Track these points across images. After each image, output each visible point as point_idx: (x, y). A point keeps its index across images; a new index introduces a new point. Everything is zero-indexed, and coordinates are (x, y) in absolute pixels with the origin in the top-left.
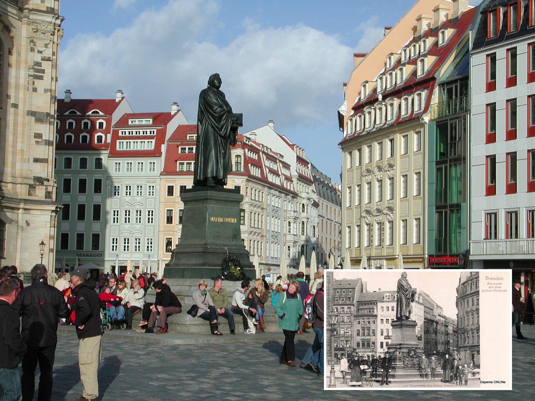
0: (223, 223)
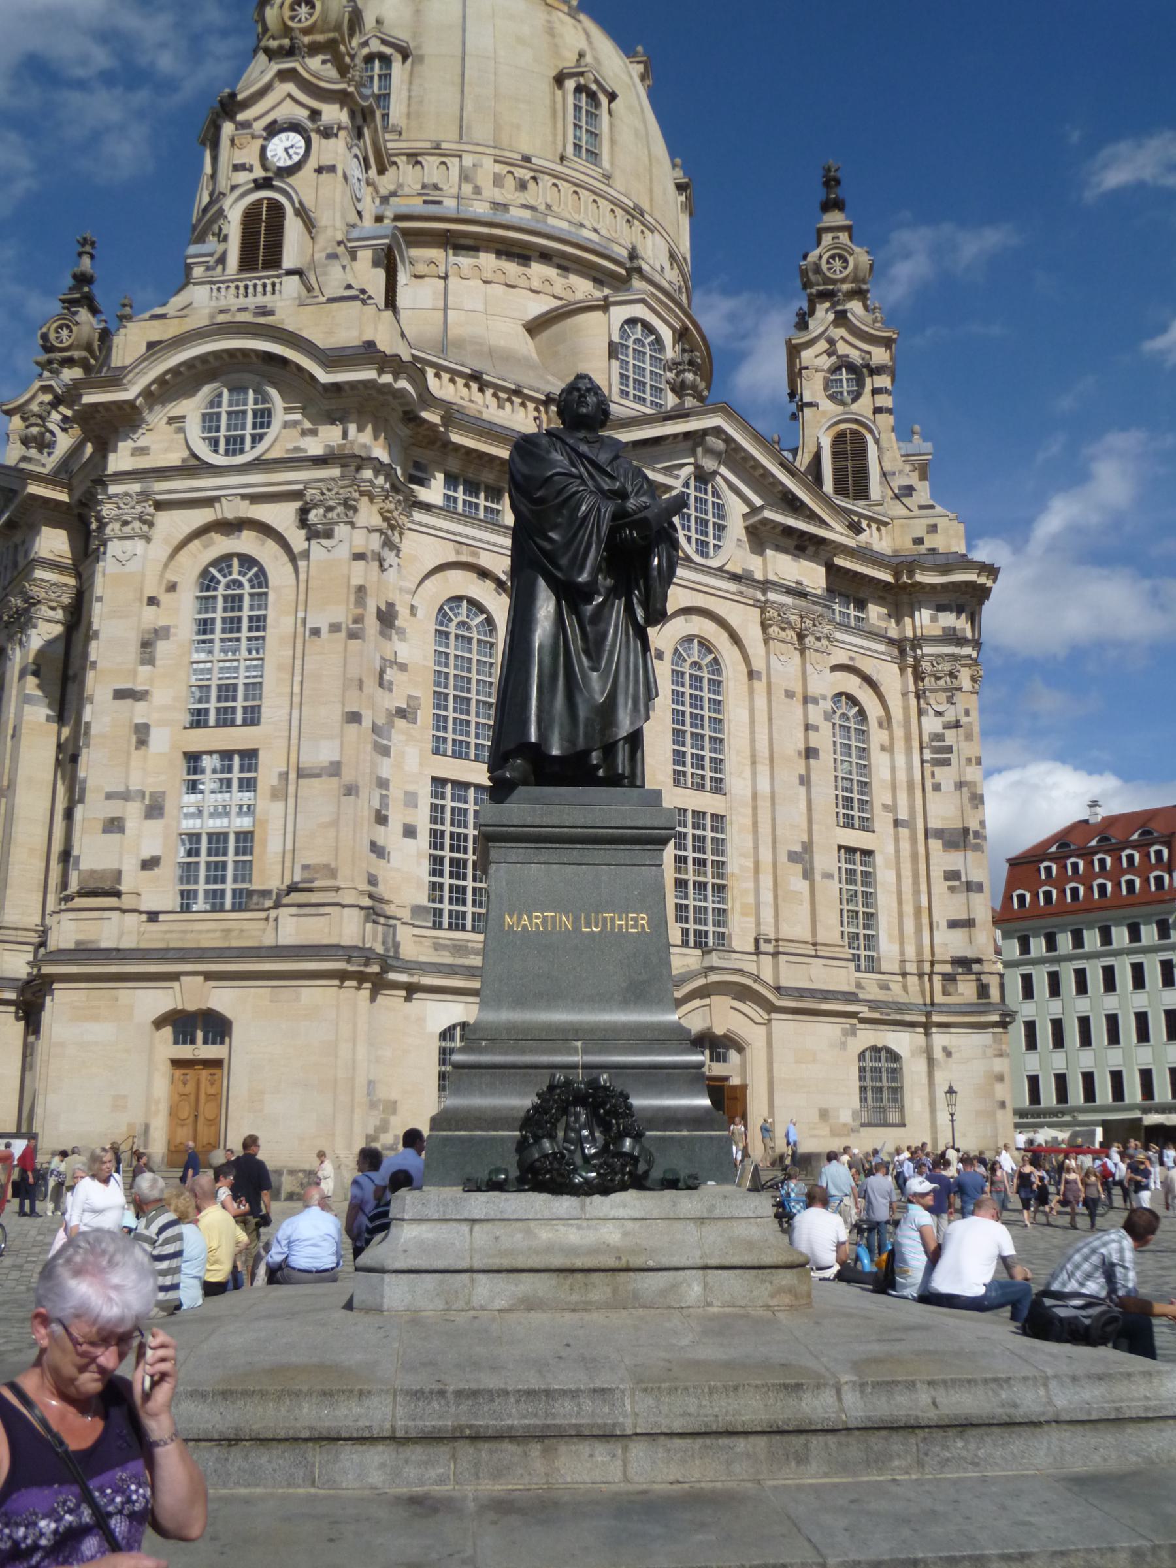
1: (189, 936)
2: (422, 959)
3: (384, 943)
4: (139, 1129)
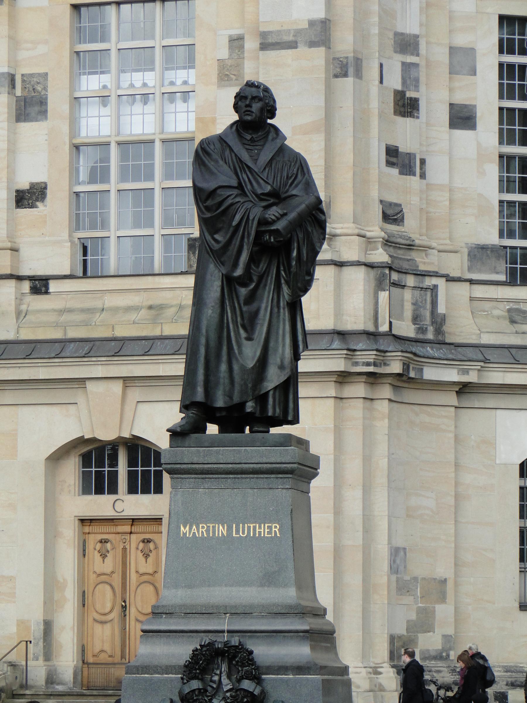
0: (228, 540)
1: (98, 318)
2: (486, 339)
3: (416, 319)
4: (36, 630)
